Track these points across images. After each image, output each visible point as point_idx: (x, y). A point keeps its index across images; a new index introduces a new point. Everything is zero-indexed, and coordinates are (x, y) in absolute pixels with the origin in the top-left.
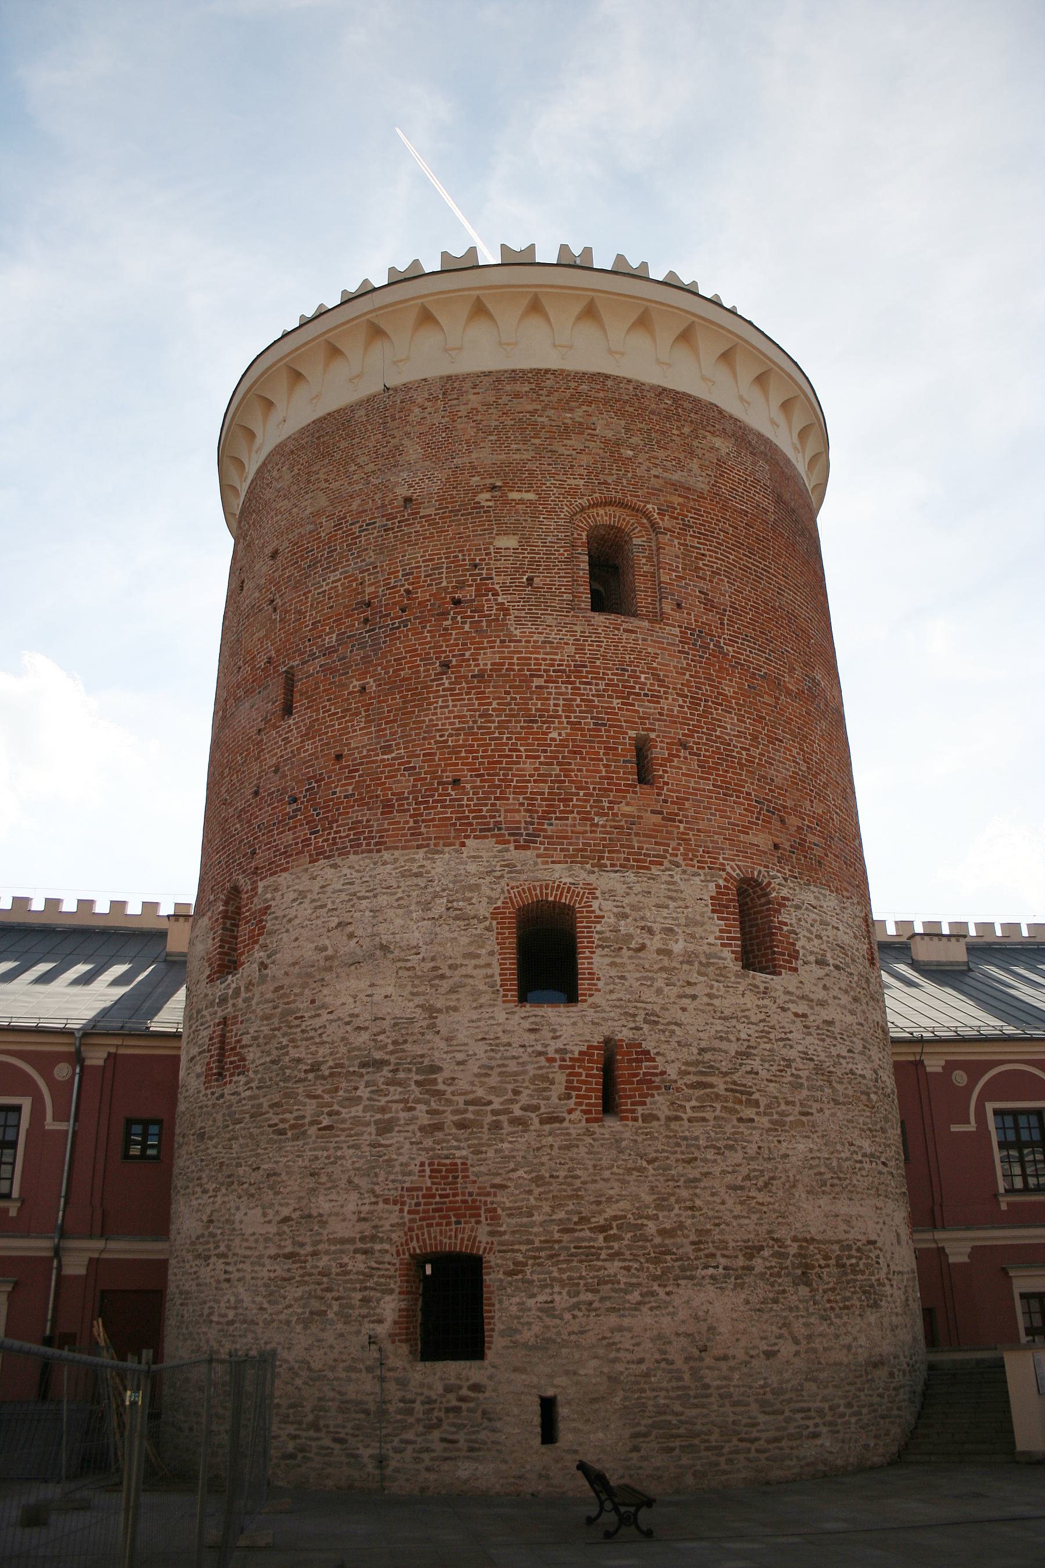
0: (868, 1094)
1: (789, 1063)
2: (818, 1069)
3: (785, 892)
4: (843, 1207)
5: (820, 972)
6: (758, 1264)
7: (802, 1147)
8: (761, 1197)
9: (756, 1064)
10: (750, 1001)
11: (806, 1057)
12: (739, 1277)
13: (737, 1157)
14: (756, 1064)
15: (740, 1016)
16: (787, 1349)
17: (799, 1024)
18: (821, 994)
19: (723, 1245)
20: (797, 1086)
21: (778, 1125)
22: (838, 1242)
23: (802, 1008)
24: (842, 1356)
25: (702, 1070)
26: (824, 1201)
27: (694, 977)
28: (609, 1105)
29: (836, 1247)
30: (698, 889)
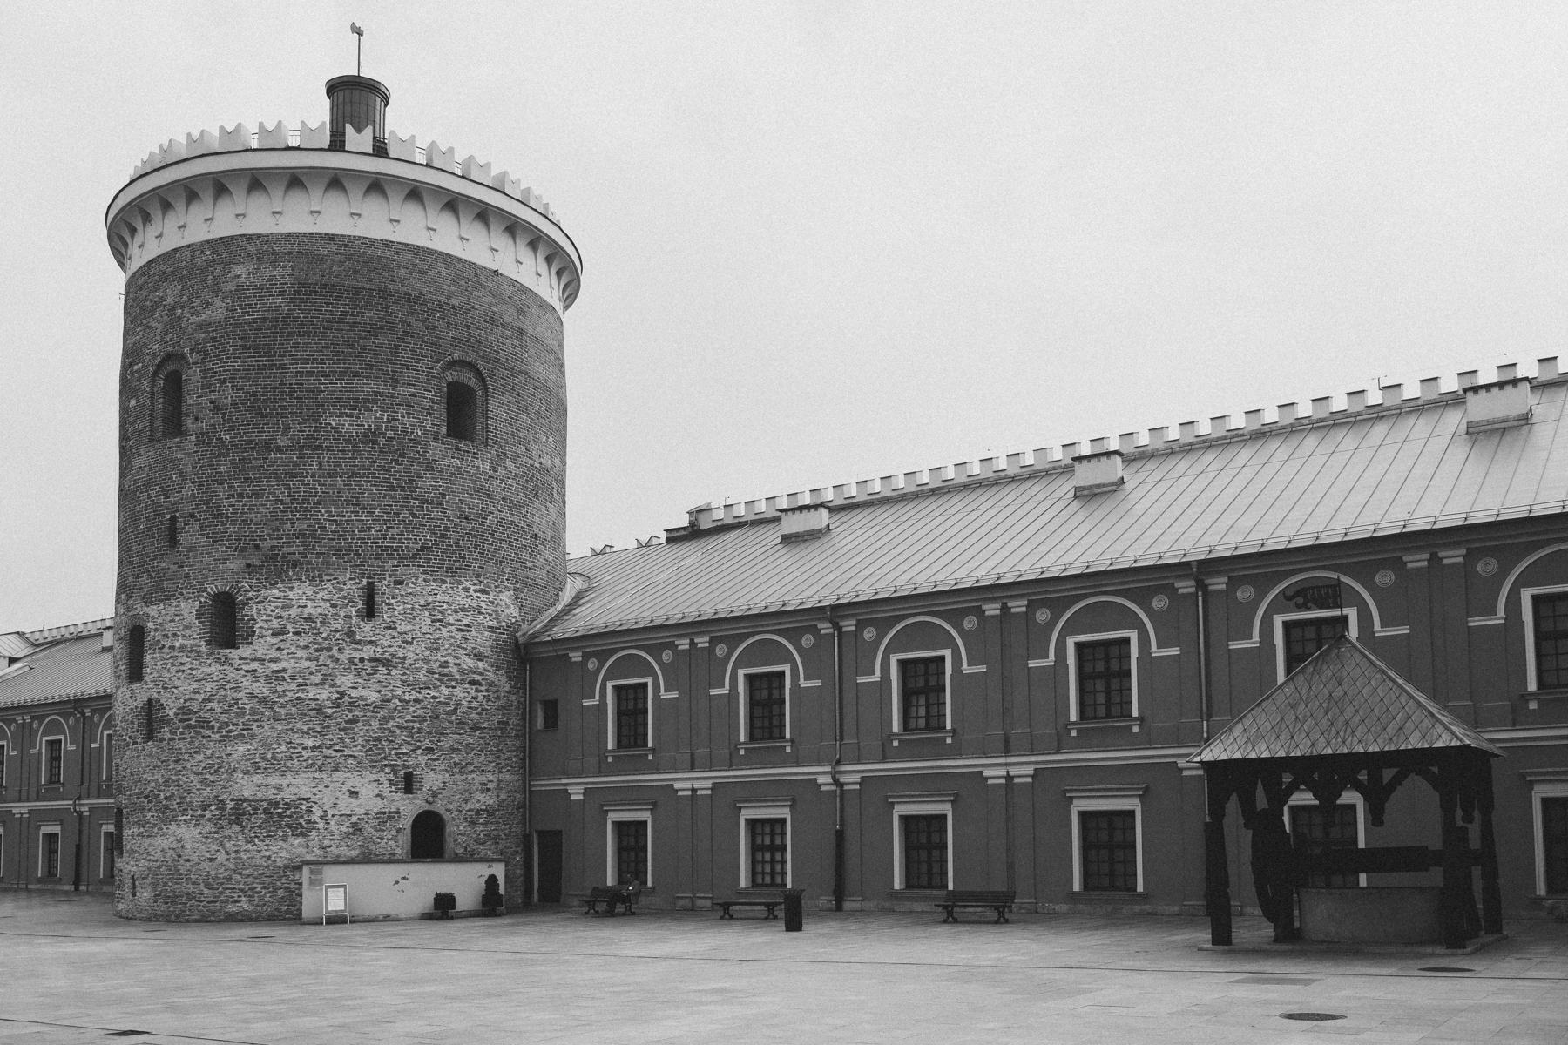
0: (319, 710)
1: (237, 701)
2: (263, 701)
3: (250, 595)
4: (274, 780)
5: (275, 641)
6: (208, 814)
7: (242, 748)
8: (212, 778)
9: (214, 705)
10: (215, 668)
11: (252, 695)
12: (198, 821)
13: (200, 757)
14: (214, 705)
15: (210, 677)
16: (221, 857)
17: (249, 677)
18: (273, 654)
19: (190, 804)
20: (241, 714)
21: (226, 738)
22: (270, 802)
23: (255, 665)
24: (263, 862)
25: (185, 712)
26: (257, 779)
27: (185, 659)
28: (150, 736)
29: (265, 804)
30: (189, 608)
